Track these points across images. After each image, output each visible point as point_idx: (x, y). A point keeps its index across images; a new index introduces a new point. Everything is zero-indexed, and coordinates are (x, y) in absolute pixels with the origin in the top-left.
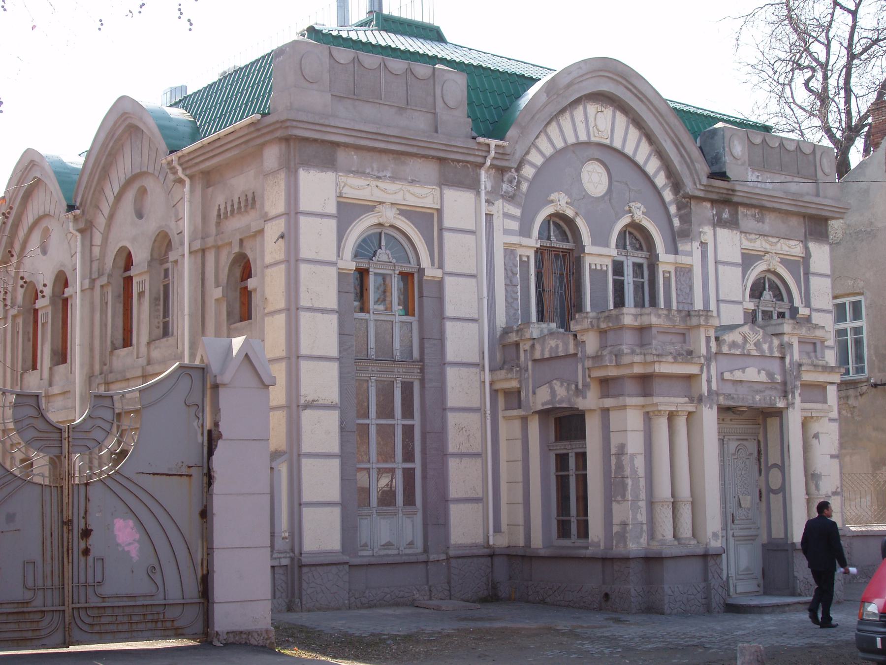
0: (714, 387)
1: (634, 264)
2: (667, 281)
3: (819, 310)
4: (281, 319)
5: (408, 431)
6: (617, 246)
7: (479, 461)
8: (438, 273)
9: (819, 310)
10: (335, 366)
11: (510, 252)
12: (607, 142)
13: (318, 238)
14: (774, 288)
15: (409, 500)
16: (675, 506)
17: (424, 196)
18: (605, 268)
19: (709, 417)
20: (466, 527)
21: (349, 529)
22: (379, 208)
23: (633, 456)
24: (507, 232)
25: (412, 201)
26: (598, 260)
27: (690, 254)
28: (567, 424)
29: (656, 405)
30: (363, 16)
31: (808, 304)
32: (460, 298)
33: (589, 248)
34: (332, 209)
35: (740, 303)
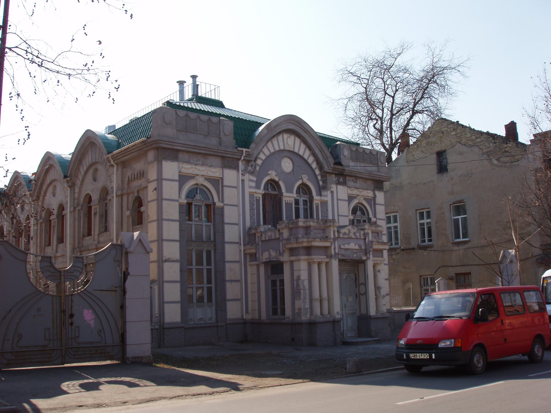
0: (337, 251)
1: (304, 201)
2: (317, 207)
3: (380, 219)
4: (155, 224)
5: (209, 271)
6: (296, 193)
7: (239, 283)
8: (222, 204)
9: (380, 219)
10: (178, 244)
11: (251, 195)
12: (292, 150)
13: (170, 190)
14: (361, 210)
15: (210, 300)
16: (321, 301)
17: (215, 172)
19: (335, 264)
20: (233, 311)
21: (184, 313)
22: (197, 177)
23: (303, 281)
24: (250, 187)
25: (210, 174)
26: (288, 199)
27: (326, 196)
28: (276, 268)
29: (313, 259)
30: (190, 97)
31: (375, 217)
32: (231, 215)
34: (176, 177)
35: (347, 216)
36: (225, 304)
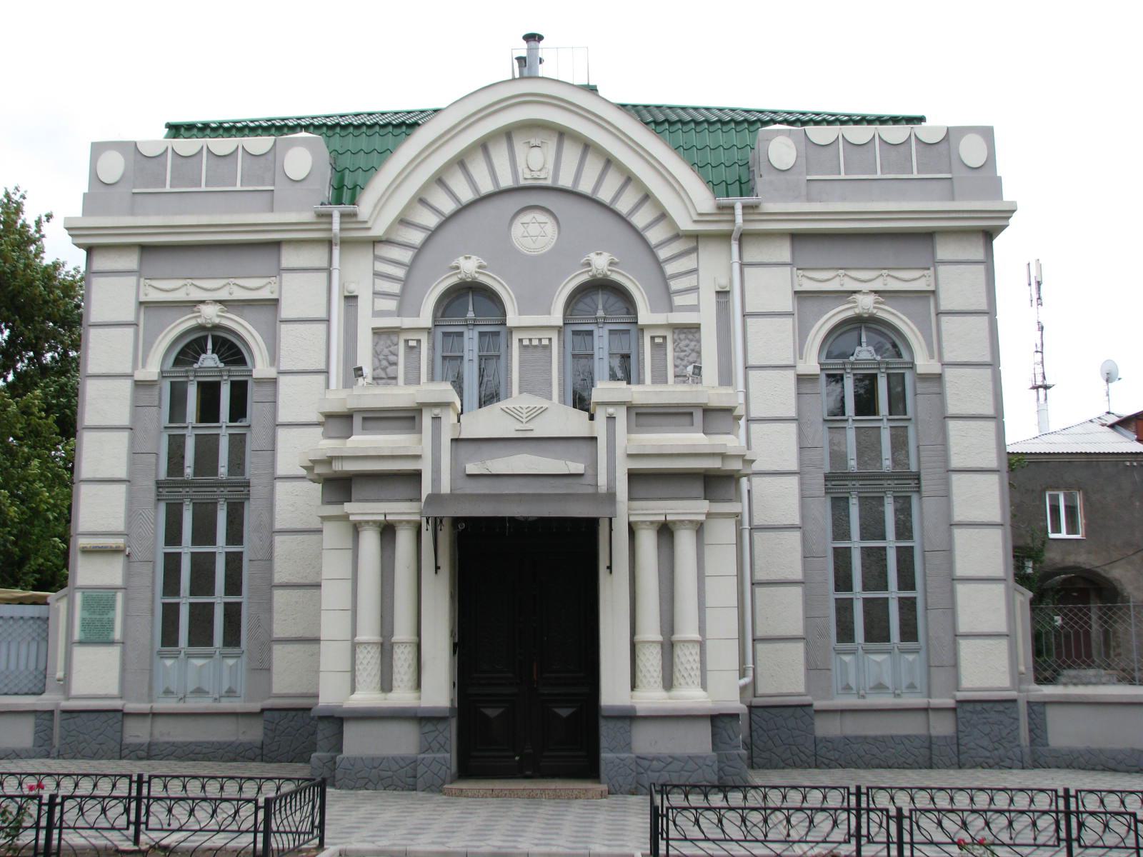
5: (234, 562)
8: (271, 373)
12: (549, 182)
18: (545, 342)
24: (377, 314)
27: (695, 308)
32: (299, 400)
33: (513, 319)
35: (793, 367)
36: (270, 650)
